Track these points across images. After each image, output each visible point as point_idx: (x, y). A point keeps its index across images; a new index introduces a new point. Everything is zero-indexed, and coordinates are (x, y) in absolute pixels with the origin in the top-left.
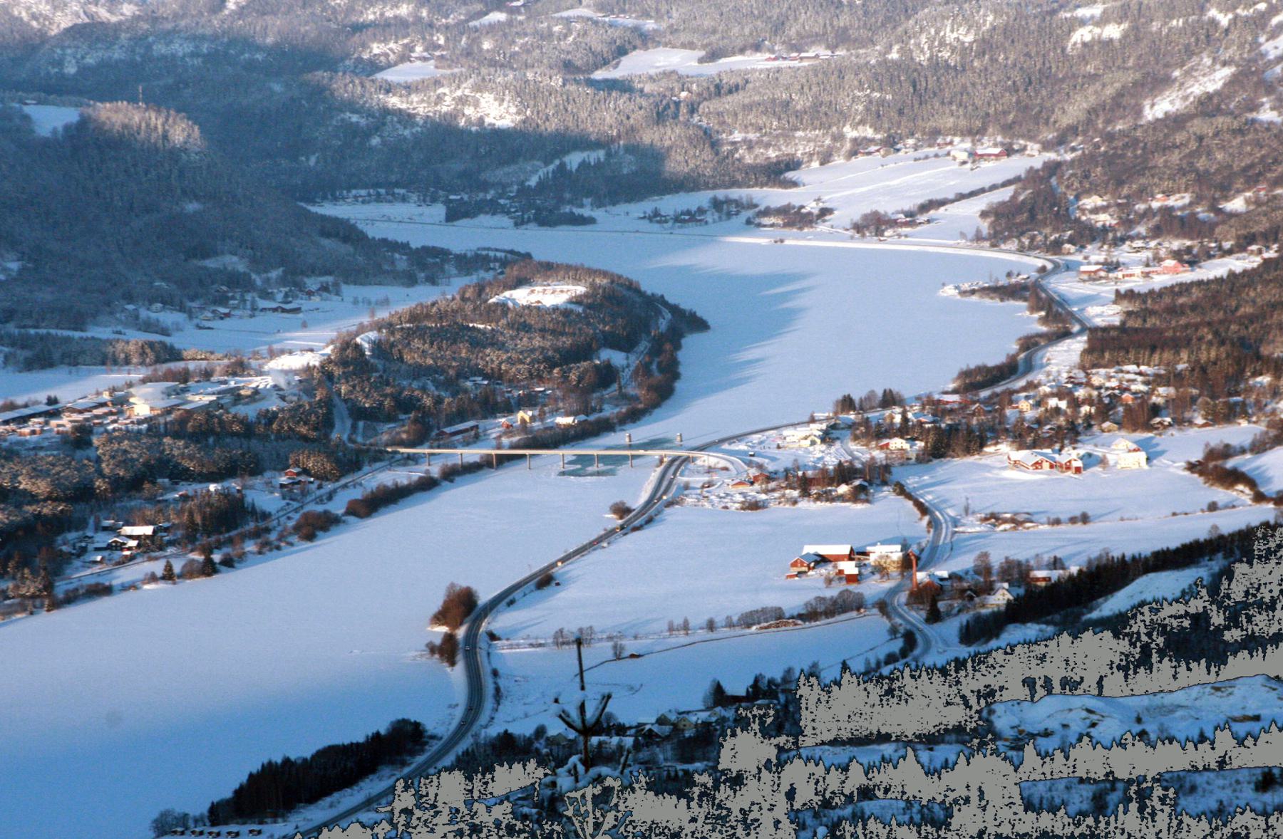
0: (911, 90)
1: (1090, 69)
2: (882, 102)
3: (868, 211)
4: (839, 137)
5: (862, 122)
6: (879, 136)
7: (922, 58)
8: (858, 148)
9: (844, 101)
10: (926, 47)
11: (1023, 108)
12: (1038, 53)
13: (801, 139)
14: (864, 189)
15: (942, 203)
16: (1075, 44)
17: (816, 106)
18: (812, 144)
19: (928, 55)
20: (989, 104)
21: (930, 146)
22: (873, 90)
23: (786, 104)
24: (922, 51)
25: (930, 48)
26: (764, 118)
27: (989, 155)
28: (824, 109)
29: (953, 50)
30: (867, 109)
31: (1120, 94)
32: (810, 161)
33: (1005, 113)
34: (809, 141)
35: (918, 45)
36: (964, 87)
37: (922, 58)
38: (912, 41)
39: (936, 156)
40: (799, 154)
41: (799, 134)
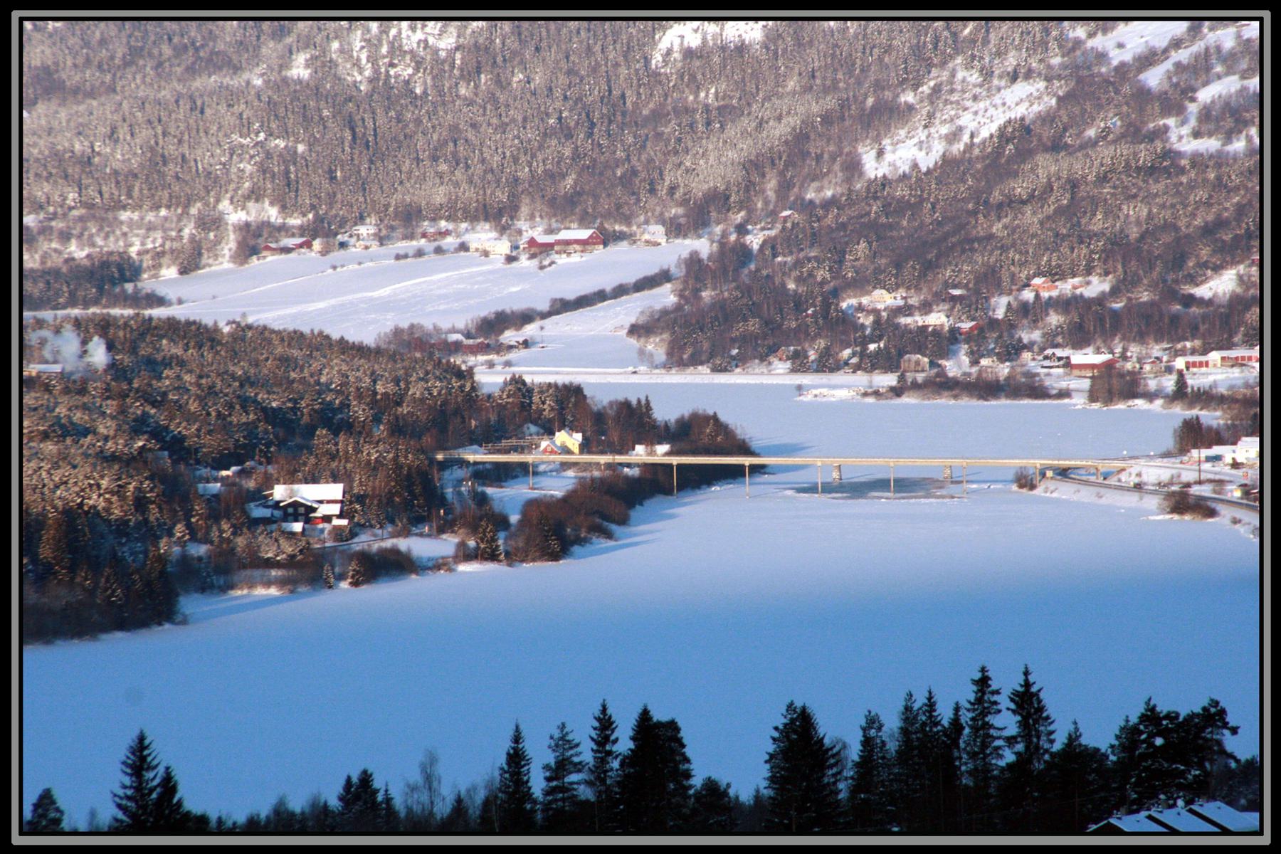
0: (348, 135)
1: (709, 95)
2: (290, 157)
3: (405, 325)
4: (211, 222)
5: (256, 194)
6: (295, 221)
7: (360, 78)
8: (253, 242)
9: (207, 157)
10: (364, 56)
11: (592, 169)
12: (594, 70)
13: (131, 223)
14: (321, 305)
15: (526, 317)
16: (669, 52)
17: (156, 160)
18: (158, 235)
19: (368, 73)
20: (516, 160)
21: (411, 237)
22: (270, 134)
23: (86, 162)
24: (357, 64)
25: (373, 59)
26: (47, 187)
27: (568, 243)
28: (171, 169)
29: (418, 64)
30: (263, 170)
31: (800, 138)
32: (157, 266)
33: (554, 176)
34: (151, 228)
35: (346, 52)
36: (454, 128)
37: (360, 78)
38: (335, 45)
39: (420, 253)
40: (133, 251)
41: (124, 216)
